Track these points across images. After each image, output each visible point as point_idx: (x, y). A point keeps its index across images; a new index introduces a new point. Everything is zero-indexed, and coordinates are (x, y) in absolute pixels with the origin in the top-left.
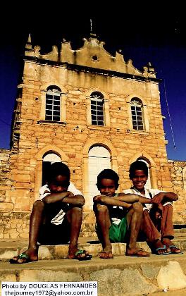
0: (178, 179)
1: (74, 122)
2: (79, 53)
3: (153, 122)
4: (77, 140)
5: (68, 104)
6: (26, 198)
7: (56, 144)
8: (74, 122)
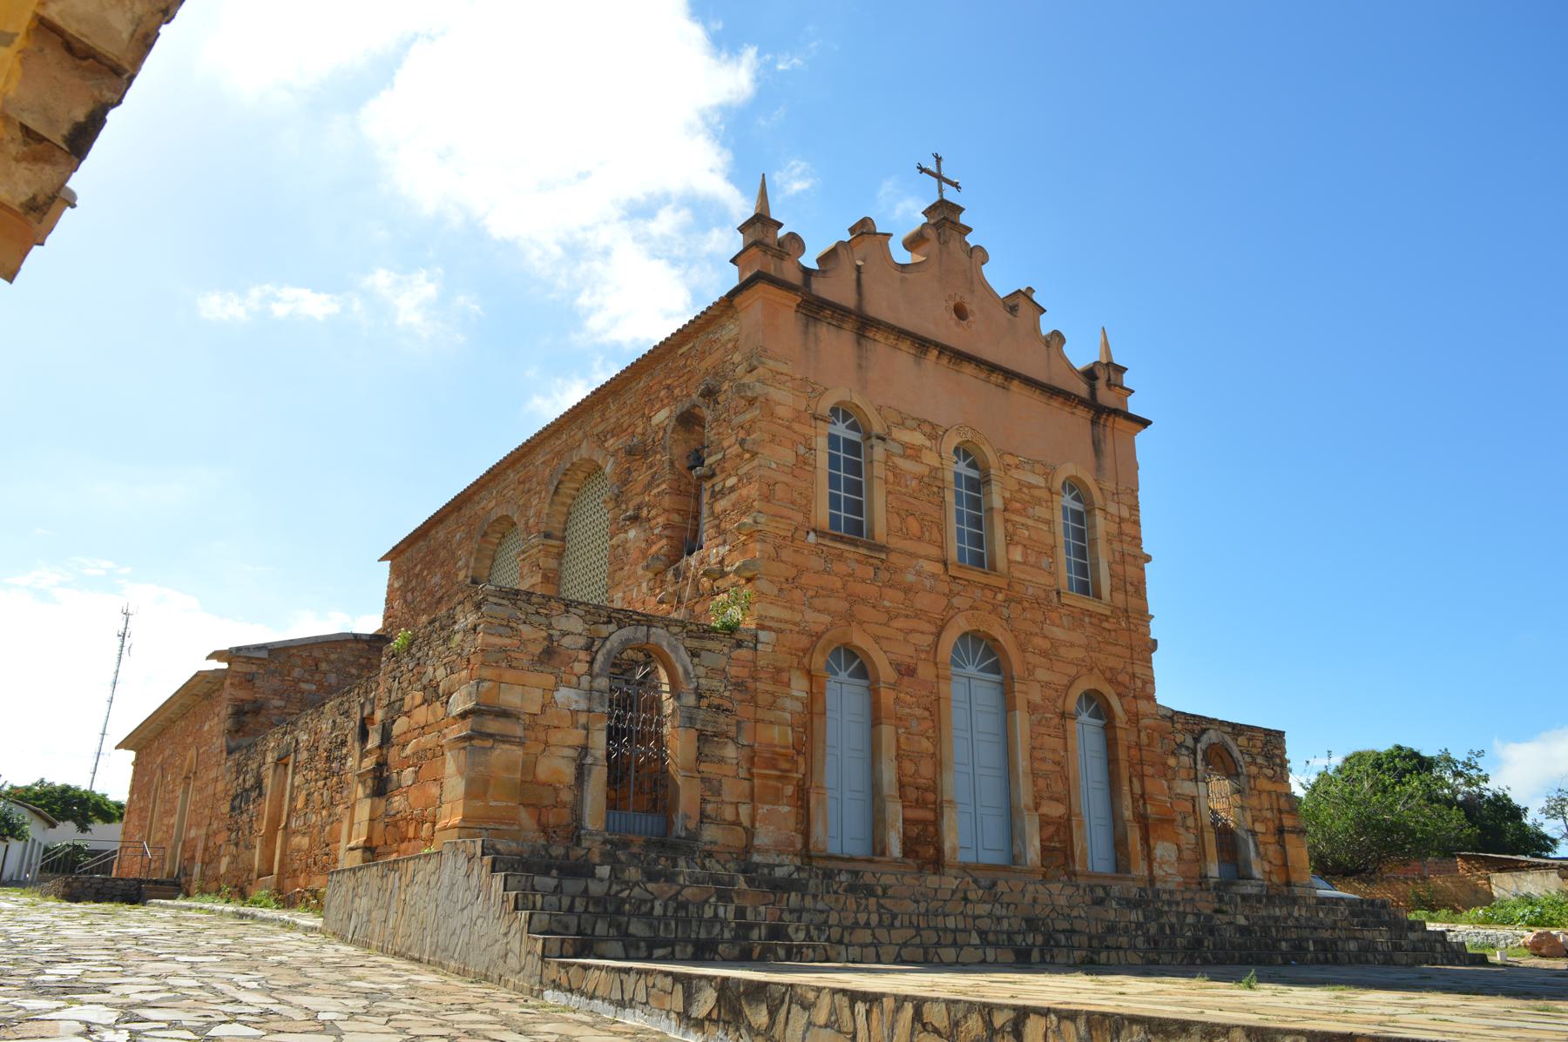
1: (909, 545)
3: (1119, 568)
4: (919, 614)
5: (890, 474)
6: (786, 809)
7: (861, 623)
8: (909, 545)
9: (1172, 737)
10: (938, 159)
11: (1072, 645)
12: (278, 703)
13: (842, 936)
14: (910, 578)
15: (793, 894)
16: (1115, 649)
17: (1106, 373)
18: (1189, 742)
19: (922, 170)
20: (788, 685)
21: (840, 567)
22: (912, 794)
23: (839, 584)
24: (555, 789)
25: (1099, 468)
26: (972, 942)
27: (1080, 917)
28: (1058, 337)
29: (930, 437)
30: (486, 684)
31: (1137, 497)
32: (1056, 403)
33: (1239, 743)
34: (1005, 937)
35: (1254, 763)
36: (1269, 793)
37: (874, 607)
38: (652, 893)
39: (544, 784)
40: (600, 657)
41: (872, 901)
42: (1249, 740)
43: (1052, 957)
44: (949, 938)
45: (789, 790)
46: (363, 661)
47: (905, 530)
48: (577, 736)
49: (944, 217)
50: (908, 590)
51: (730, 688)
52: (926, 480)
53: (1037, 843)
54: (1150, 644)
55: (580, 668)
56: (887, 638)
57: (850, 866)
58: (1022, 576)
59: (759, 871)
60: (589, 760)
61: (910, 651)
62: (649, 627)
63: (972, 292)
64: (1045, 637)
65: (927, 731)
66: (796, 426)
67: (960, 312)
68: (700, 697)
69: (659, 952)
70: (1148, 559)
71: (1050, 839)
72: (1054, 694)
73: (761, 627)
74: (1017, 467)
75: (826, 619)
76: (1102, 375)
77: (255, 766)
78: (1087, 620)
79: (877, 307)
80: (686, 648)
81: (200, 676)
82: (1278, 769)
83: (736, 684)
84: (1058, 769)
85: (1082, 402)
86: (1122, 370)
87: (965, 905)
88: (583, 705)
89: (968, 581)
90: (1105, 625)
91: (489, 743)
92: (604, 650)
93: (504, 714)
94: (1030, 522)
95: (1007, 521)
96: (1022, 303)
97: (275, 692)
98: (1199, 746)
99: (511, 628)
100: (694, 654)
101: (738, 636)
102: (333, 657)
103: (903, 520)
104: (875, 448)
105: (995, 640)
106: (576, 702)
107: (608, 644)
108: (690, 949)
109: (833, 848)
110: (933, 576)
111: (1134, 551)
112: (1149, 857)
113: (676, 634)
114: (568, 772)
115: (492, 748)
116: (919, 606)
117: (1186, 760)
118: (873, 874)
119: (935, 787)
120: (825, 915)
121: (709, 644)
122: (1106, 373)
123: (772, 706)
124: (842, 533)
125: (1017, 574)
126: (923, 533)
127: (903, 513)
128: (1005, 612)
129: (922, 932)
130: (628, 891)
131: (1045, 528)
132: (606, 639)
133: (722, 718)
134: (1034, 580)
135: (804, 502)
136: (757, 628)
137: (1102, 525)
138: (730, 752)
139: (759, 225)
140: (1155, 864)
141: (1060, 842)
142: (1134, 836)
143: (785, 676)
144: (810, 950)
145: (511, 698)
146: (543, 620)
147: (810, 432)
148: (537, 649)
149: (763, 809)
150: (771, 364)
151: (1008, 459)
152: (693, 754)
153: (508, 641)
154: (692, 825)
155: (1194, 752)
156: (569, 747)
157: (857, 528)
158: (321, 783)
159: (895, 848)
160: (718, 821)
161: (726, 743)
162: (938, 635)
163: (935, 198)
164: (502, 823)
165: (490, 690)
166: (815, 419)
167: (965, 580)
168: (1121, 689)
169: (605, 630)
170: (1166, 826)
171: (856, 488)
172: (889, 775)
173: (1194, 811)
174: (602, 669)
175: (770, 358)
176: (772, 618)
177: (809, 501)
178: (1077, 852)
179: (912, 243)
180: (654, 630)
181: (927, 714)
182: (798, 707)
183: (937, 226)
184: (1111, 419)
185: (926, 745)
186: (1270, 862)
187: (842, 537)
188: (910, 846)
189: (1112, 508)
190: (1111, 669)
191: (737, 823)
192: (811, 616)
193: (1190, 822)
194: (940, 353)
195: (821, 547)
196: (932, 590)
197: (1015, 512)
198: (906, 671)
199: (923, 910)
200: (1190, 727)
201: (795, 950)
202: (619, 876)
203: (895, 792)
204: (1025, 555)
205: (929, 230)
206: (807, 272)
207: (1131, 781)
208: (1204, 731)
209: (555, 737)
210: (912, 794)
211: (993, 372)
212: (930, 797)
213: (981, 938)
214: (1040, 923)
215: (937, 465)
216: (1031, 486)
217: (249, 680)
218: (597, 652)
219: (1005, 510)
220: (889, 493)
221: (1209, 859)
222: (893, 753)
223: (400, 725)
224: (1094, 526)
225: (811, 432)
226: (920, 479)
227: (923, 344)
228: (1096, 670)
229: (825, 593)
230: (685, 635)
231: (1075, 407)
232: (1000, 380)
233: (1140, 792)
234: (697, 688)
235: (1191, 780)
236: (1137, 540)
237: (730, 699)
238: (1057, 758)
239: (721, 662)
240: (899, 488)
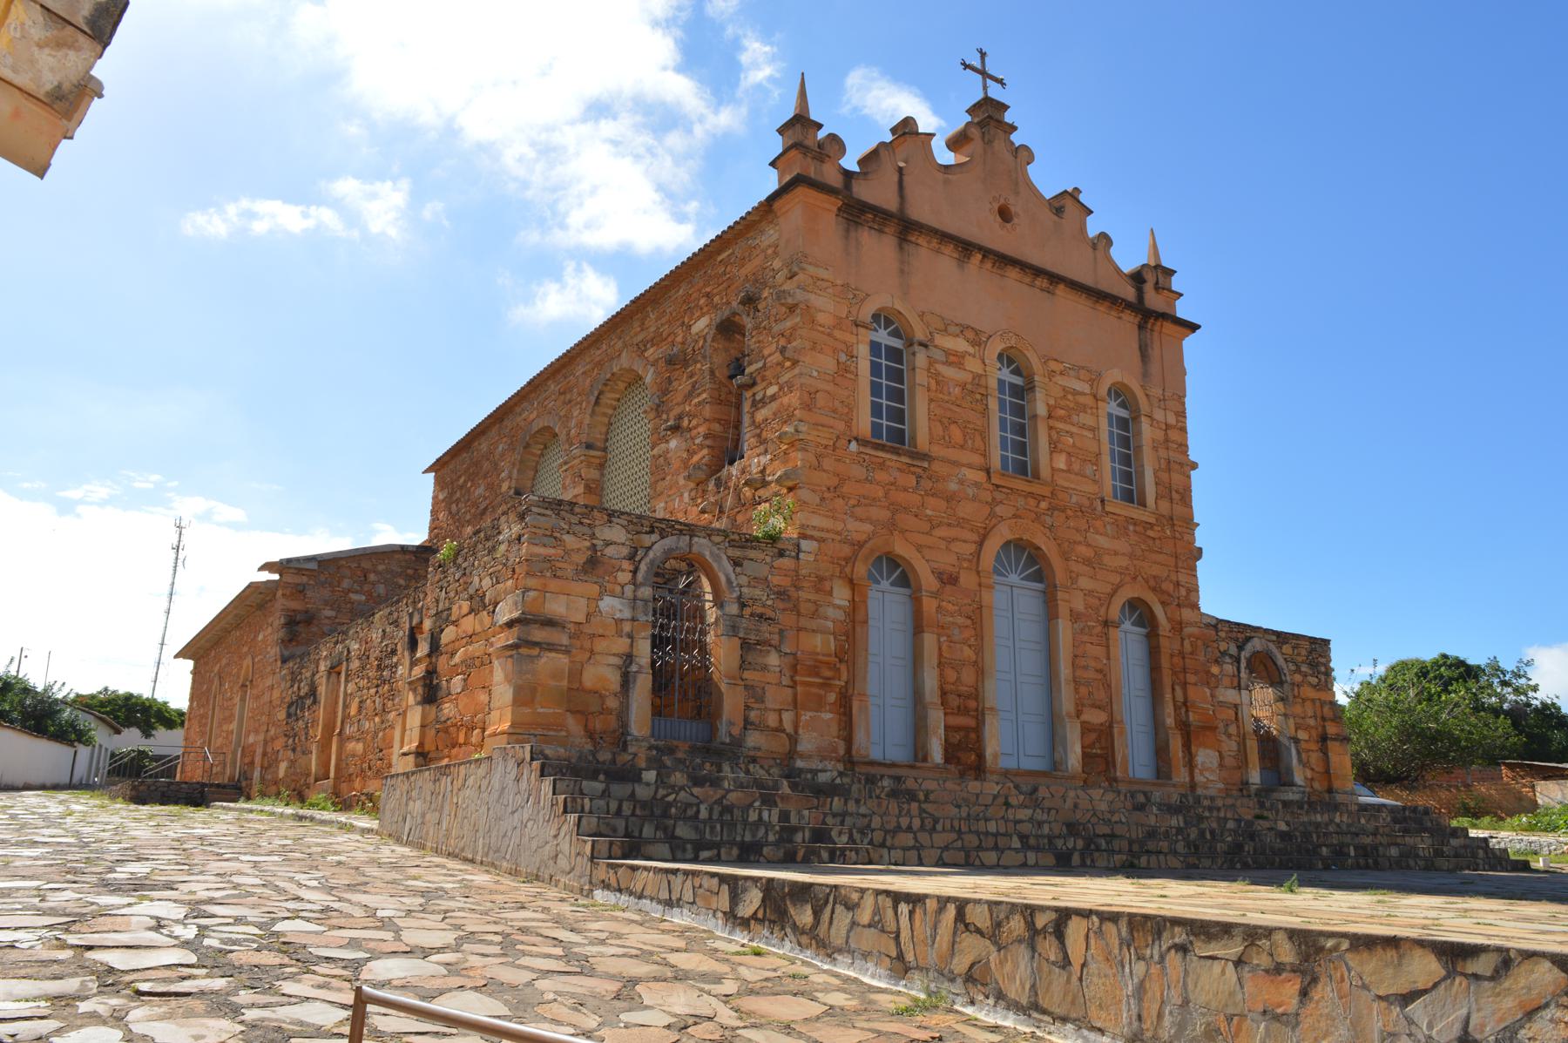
3: (1164, 476)
4: (961, 523)
5: (933, 382)
6: (828, 716)
7: (903, 532)
10: (983, 55)
11: (1116, 553)
12: (329, 613)
13: (885, 840)
14: (953, 486)
15: (836, 799)
16: (1160, 558)
17: (1154, 276)
18: (1233, 650)
19: (966, 66)
20: (830, 593)
21: (881, 476)
22: (954, 701)
23: (881, 494)
24: (602, 697)
25: (1145, 374)
26: (1013, 846)
27: (1121, 822)
28: (1105, 239)
29: (974, 343)
30: (532, 594)
31: (1184, 404)
32: (1102, 308)
33: (1284, 651)
34: (1046, 841)
35: (1298, 671)
36: (1313, 701)
37: (916, 516)
38: (697, 797)
39: (590, 691)
40: (643, 567)
41: (914, 805)
42: (1294, 648)
43: (1092, 861)
44: (990, 842)
45: (832, 697)
46: (410, 572)
47: (947, 438)
48: (622, 645)
50: (950, 498)
51: (773, 597)
52: (969, 387)
53: (1078, 749)
55: (624, 577)
56: (930, 547)
57: (894, 772)
58: (1066, 484)
59: (803, 776)
60: (634, 668)
61: (952, 559)
62: (691, 536)
63: (1017, 193)
64: (1088, 545)
65: (969, 639)
66: (837, 333)
67: (1005, 214)
68: (743, 605)
69: (705, 854)
70: (1194, 466)
71: (1092, 746)
72: (1097, 602)
73: (803, 536)
74: (1061, 373)
75: (868, 527)
76: (1150, 278)
77: (308, 674)
78: (1131, 528)
79: (920, 211)
80: (728, 557)
81: (253, 588)
82: (1323, 678)
83: (779, 593)
84: (1100, 676)
85: (1129, 306)
86: (1171, 272)
87: (1006, 810)
88: (627, 614)
89: (1011, 489)
90: (1150, 533)
91: (535, 651)
92: (647, 560)
93: (550, 623)
94: (1074, 430)
95: (1051, 428)
96: (1068, 204)
97: (326, 603)
98: (1243, 653)
99: (555, 538)
100: (736, 563)
101: (780, 546)
102: (381, 568)
103: (945, 428)
104: (918, 355)
105: (1038, 548)
106: (620, 611)
107: (651, 554)
108: (735, 851)
109: (876, 754)
110: (976, 484)
111: (1179, 458)
112: (1190, 764)
113: (718, 544)
114: (614, 679)
115: (539, 656)
116: (961, 515)
117: (1229, 668)
118: (915, 779)
119: (976, 694)
120: (867, 820)
121: (752, 554)
122: (1154, 276)
123: (815, 615)
125: (1061, 482)
126: (966, 441)
127: (945, 421)
128: (1048, 520)
129: (963, 836)
130: (673, 796)
131: (1090, 435)
132: (649, 548)
133: (765, 627)
134: (1078, 487)
135: (846, 410)
136: (799, 538)
137: (1147, 432)
138: (773, 660)
139: (798, 127)
140: (1197, 771)
141: (1102, 748)
142: (1176, 744)
143: (827, 585)
144: (853, 853)
145: (556, 607)
146: (586, 530)
147: (852, 339)
148: (580, 559)
149: (806, 716)
150: (811, 269)
151: (1053, 365)
152: (736, 662)
153: (552, 551)
154: (736, 731)
155: (1238, 661)
156: (614, 655)
157: (898, 436)
159: (937, 753)
160: (761, 727)
161: (769, 652)
162: (981, 544)
163: (980, 96)
164: (550, 730)
165: (535, 599)
166: (857, 326)
167: (1008, 488)
168: (1165, 598)
169: (647, 540)
170: (1208, 733)
171: (897, 395)
172: (931, 682)
173: (1237, 719)
174: (645, 579)
175: (810, 264)
176: (814, 527)
177: (851, 409)
178: (1119, 758)
179: (954, 143)
180: (696, 539)
181: (969, 622)
182: (840, 615)
183: (981, 125)
184: (1159, 324)
185: (968, 653)
186: (1312, 769)
187: (884, 446)
188: (952, 753)
189: (1159, 415)
190: (1155, 577)
191: (780, 729)
192: (852, 525)
193: (1233, 729)
194: (984, 256)
195: (863, 456)
196: (974, 499)
197: (1061, 419)
198: (948, 580)
199: (964, 815)
200: (1234, 635)
201: (838, 853)
202: (665, 780)
204: (1069, 463)
205: (973, 130)
206: (848, 175)
207: (1173, 689)
208: (1248, 639)
209: (600, 645)
210: (954, 701)
211: (1038, 276)
212: (972, 704)
213: (1021, 842)
214: (1081, 828)
215: (980, 372)
216: (1075, 393)
217: (300, 591)
218: (640, 561)
219: (1050, 417)
220: (931, 400)
221: (1251, 766)
222: (935, 662)
223: (448, 634)
224: (1139, 433)
225: (853, 339)
226: (963, 386)
227: (966, 248)
228: (1139, 578)
229: (867, 501)
230: (727, 545)
231: (1122, 312)
232: (1045, 283)
234: (740, 597)
235: (1235, 688)
236: (1183, 447)
237: (773, 608)
238: (1099, 667)
239: (763, 571)
240: (941, 396)
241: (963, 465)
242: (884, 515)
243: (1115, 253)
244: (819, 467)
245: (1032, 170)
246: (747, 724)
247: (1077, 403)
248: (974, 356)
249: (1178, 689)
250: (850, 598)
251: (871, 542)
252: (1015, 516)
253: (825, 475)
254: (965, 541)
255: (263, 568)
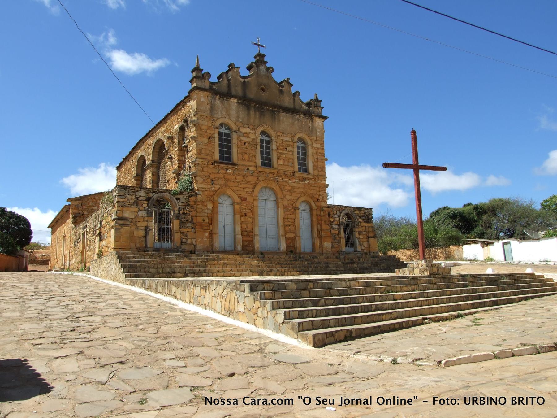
0: (335, 223)
1: (245, 163)
2: (248, 81)
3: (316, 164)
4: (248, 183)
5: (239, 143)
6: (206, 239)
7: (229, 187)
8: (245, 163)
9: (332, 212)
11: (299, 188)
18: (338, 213)
20: (206, 206)
23: (222, 176)
29: (252, 130)
36: (365, 227)
37: (233, 182)
39: (136, 237)
47: (243, 158)
49: (260, 59)
54: (326, 186)
61: (245, 193)
64: (290, 186)
69: (155, 276)
71: (290, 243)
72: (292, 202)
74: (282, 136)
75: (218, 186)
77: (78, 233)
81: (65, 207)
84: (293, 224)
86: (320, 101)
89: (264, 172)
95: (278, 152)
98: (341, 214)
103: (243, 156)
111: (322, 158)
116: (248, 180)
124: (224, 161)
125: (281, 168)
126: (249, 159)
134: (287, 169)
137: (310, 151)
141: (293, 244)
142: (317, 242)
145: (127, 215)
146: (134, 193)
148: (132, 201)
151: (279, 134)
153: (124, 200)
155: (340, 216)
158: (92, 237)
160: (185, 243)
162: (253, 189)
165: (120, 213)
169: (151, 195)
172: (238, 229)
175: (200, 112)
176: (201, 188)
179: (249, 68)
181: (250, 211)
183: (257, 62)
189: (315, 145)
190: (312, 194)
191: (192, 244)
197: (280, 150)
203: (240, 233)
204: (284, 162)
207: (317, 226)
210: (245, 233)
212: (251, 234)
215: (254, 138)
216: (286, 141)
217: (77, 207)
219: (277, 149)
220: (238, 148)
221: (342, 246)
225: (213, 132)
228: (307, 195)
233: (320, 229)
236: (323, 154)
240: (242, 146)
241: (249, 166)
242: (223, 182)
243: (301, 97)
244: (203, 170)
245: (273, 75)
246: (182, 242)
247: (287, 144)
248: (252, 133)
249: (319, 226)
250: (212, 206)
251: (219, 190)
252: (265, 180)
253: (204, 173)
254: (249, 188)
255: (68, 201)
